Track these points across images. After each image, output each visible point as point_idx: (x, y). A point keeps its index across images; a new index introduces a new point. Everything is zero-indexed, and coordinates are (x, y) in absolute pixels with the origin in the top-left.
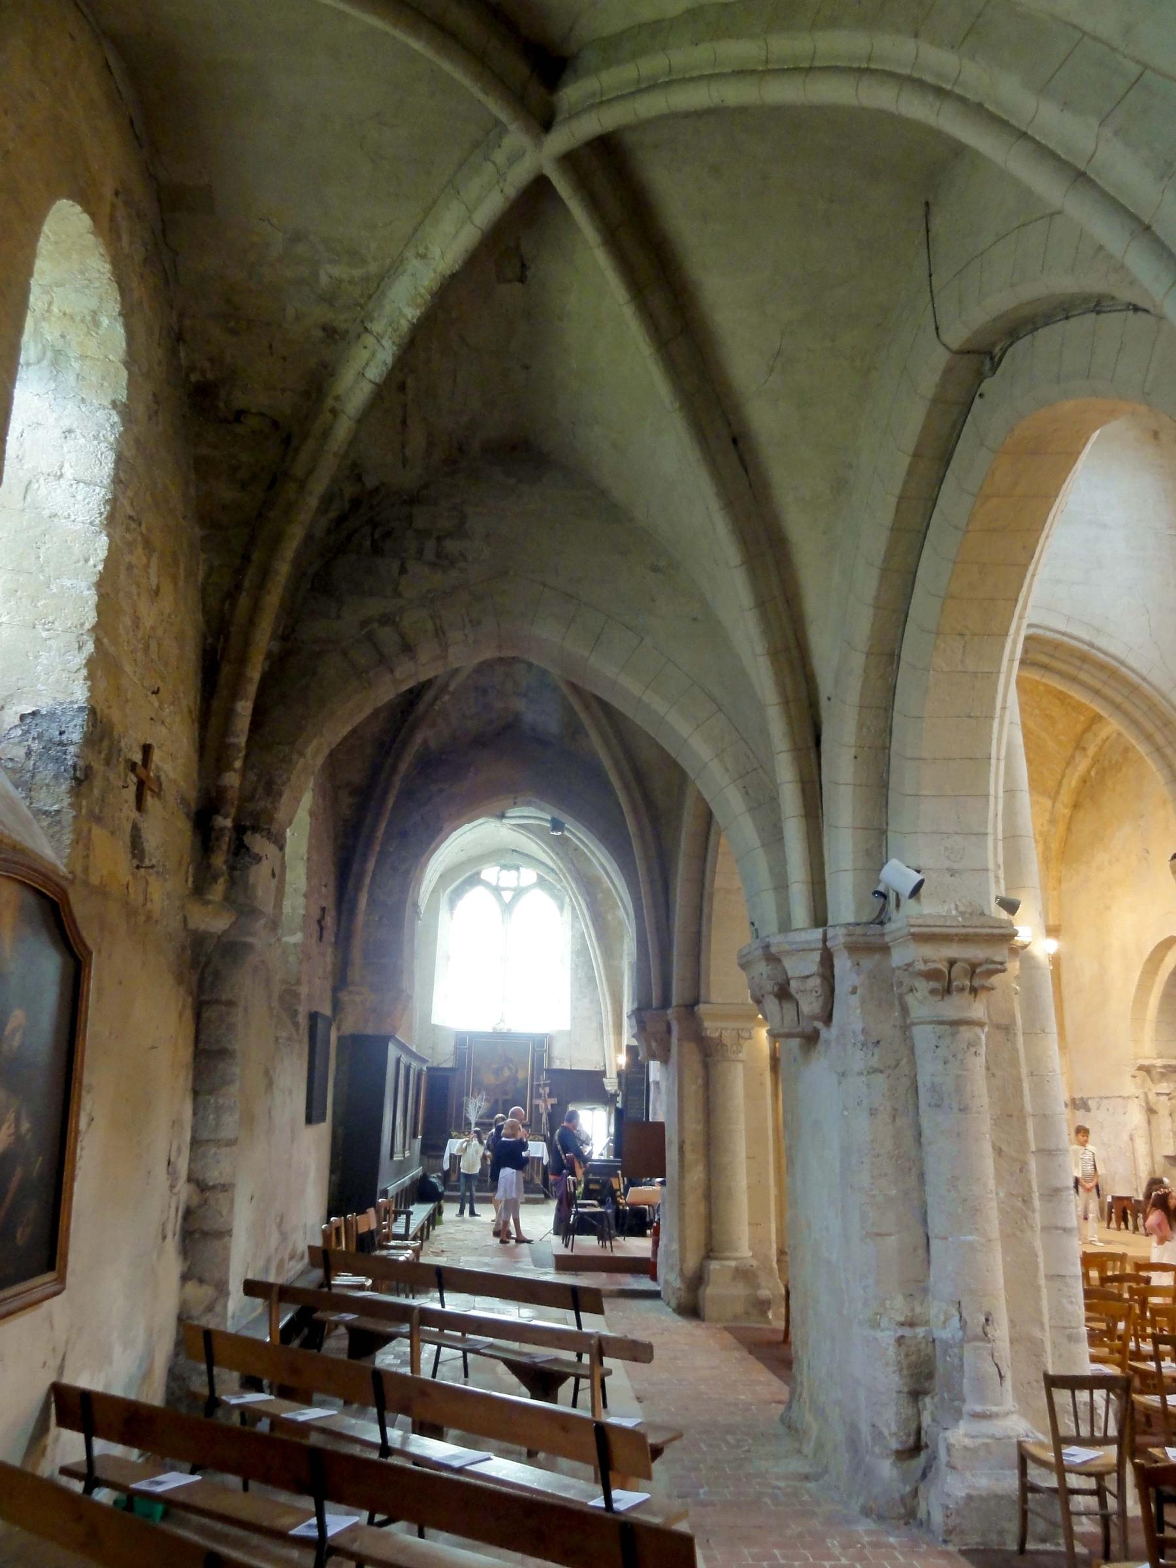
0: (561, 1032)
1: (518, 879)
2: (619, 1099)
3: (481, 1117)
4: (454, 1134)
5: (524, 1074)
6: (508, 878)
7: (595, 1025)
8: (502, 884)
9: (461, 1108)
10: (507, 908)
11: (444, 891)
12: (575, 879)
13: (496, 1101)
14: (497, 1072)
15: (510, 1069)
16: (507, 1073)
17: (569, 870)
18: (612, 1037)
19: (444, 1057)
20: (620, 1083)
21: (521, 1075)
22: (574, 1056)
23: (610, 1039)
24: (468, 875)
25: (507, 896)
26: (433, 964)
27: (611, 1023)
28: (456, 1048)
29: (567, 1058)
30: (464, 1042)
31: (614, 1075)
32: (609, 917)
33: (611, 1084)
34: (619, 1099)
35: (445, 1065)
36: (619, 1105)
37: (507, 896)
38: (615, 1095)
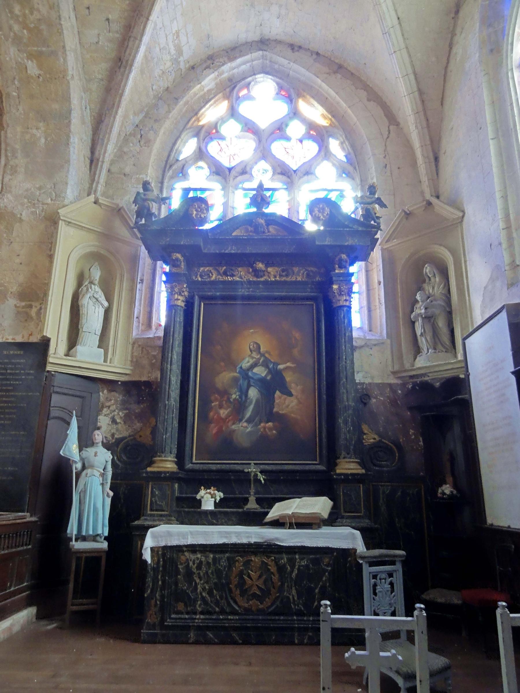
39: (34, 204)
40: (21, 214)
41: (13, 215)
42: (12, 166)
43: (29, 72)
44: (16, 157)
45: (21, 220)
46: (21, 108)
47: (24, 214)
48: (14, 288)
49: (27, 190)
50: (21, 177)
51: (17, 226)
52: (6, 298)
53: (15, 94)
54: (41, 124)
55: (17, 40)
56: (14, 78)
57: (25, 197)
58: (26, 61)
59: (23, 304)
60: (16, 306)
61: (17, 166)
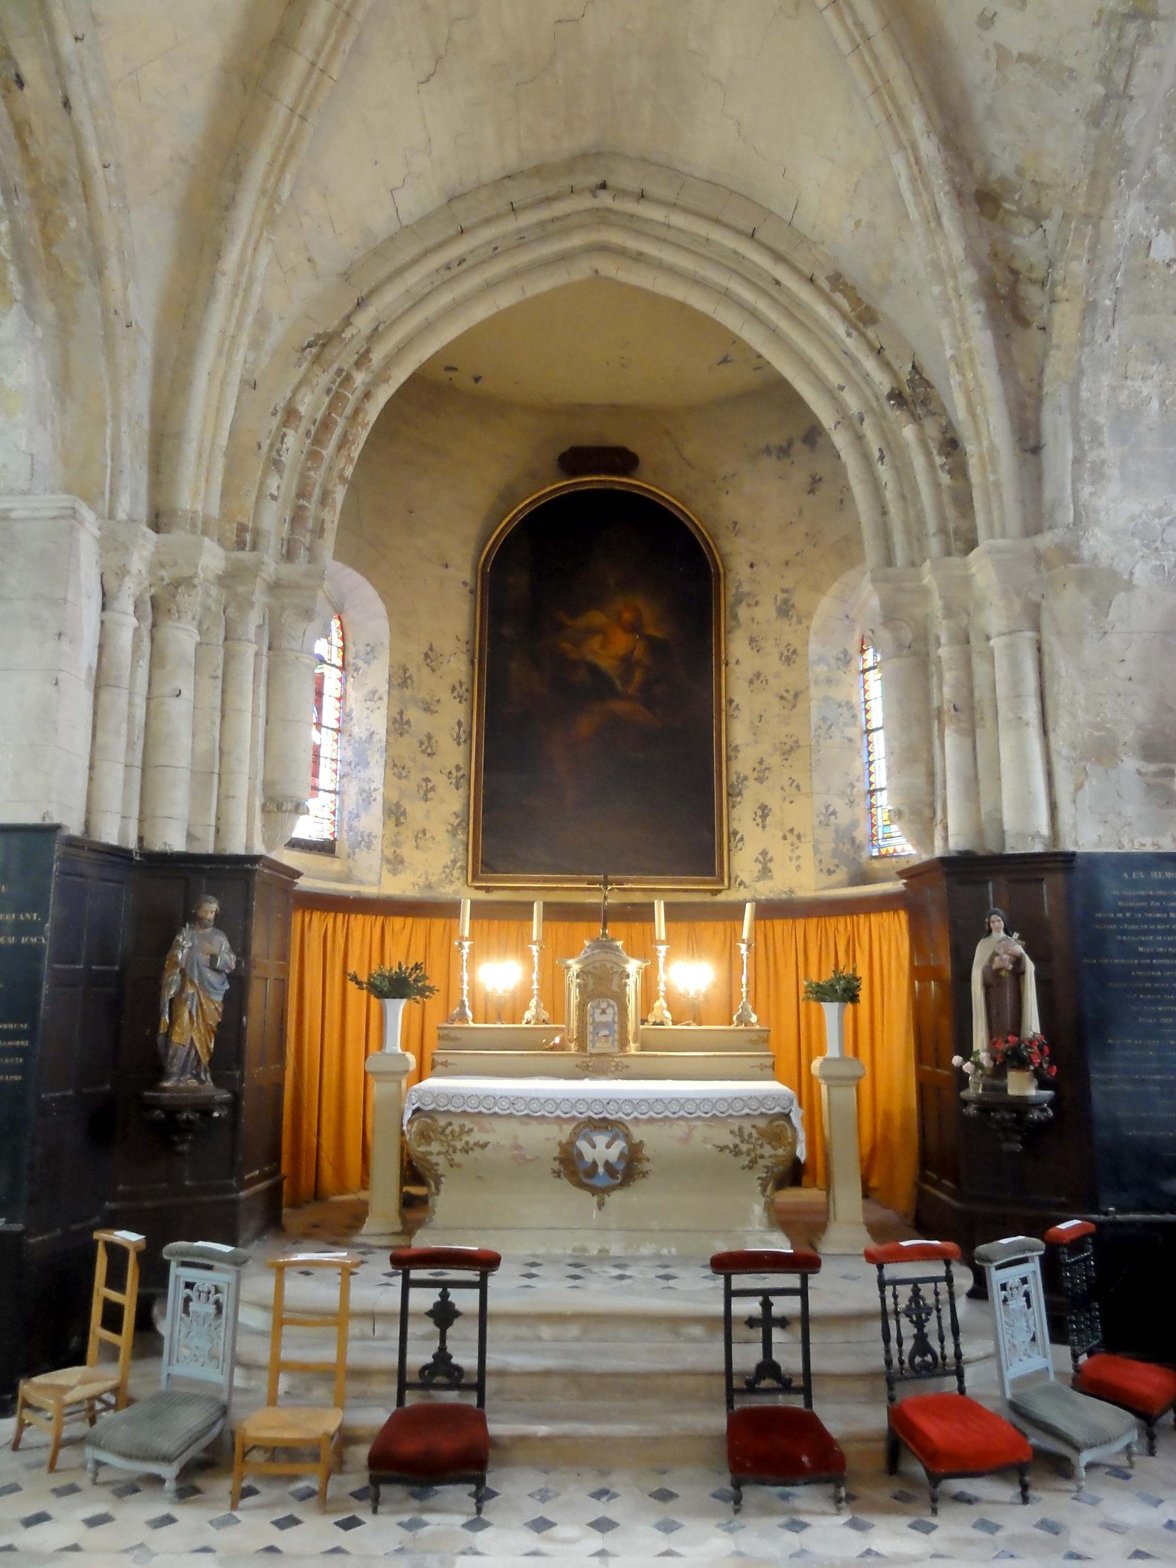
39: (1156, 549)
40: (1131, 574)
41: (1113, 574)
42: (1093, 463)
43: (1152, 254)
44: (1101, 444)
45: (1130, 586)
46: (1114, 334)
47: (1137, 571)
48: (1129, 735)
49: (1133, 518)
50: (1113, 489)
51: (1121, 597)
52: (1114, 754)
53: (1108, 302)
54: (1153, 369)
55: (1155, 189)
56: (1117, 270)
57: (1133, 535)
58: (1153, 230)
59: (1152, 768)
60: (1139, 772)
61: (1103, 462)
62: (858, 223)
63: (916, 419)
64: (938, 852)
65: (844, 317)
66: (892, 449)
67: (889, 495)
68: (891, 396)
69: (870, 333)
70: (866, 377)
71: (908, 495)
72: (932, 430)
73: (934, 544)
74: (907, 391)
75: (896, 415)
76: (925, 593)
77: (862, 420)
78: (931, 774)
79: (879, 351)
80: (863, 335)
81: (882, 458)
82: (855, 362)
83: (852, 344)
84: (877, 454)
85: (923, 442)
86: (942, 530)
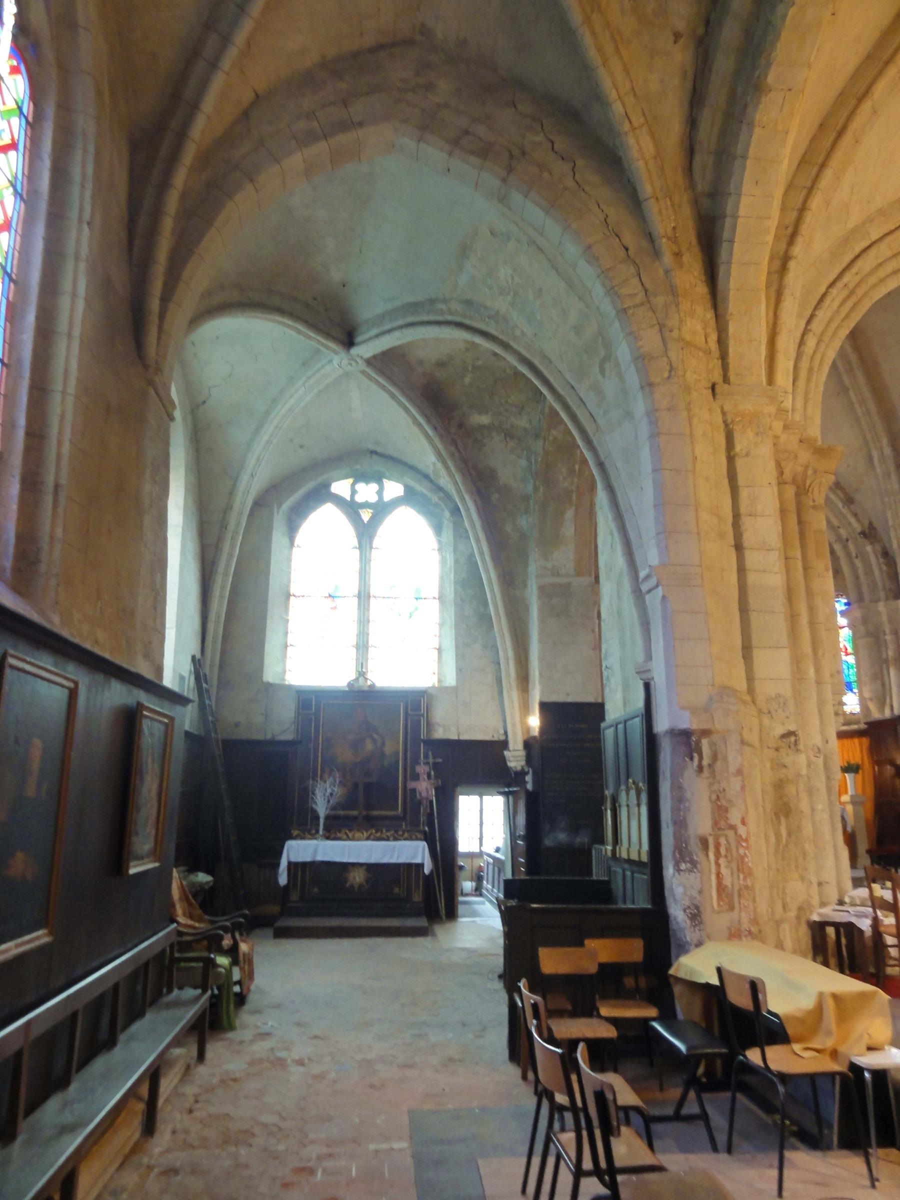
0: (442, 689)
1: (380, 493)
2: (529, 778)
3: (333, 808)
4: (295, 833)
5: (394, 746)
6: (367, 492)
7: (490, 678)
8: (359, 499)
9: (306, 795)
10: (366, 533)
11: (280, 506)
12: (460, 470)
13: (356, 785)
14: (356, 745)
15: (374, 741)
16: (369, 746)
17: (452, 455)
18: (515, 694)
19: (281, 724)
20: (529, 759)
21: (388, 749)
22: (464, 721)
23: (512, 696)
24: (311, 485)
25: (366, 515)
26: (265, 601)
27: (513, 674)
28: (298, 712)
29: (452, 724)
30: (309, 701)
31: (520, 746)
32: (508, 528)
33: (515, 758)
34: (529, 778)
35: (282, 738)
36: (529, 787)
37: (366, 515)
38: (521, 774)
62: (849, 466)
63: (872, 543)
64: (887, 714)
65: (841, 500)
66: (861, 555)
67: (861, 572)
68: (860, 533)
69: (852, 507)
70: (850, 524)
71: (869, 572)
72: (879, 548)
73: (882, 594)
74: (867, 531)
75: (861, 540)
76: (879, 613)
77: (847, 540)
78: (883, 685)
79: (855, 515)
80: (849, 508)
81: (857, 557)
82: (845, 517)
83: (845, 511)
84: (854, 555)
85: (874, 552)
86: (884, 589)
